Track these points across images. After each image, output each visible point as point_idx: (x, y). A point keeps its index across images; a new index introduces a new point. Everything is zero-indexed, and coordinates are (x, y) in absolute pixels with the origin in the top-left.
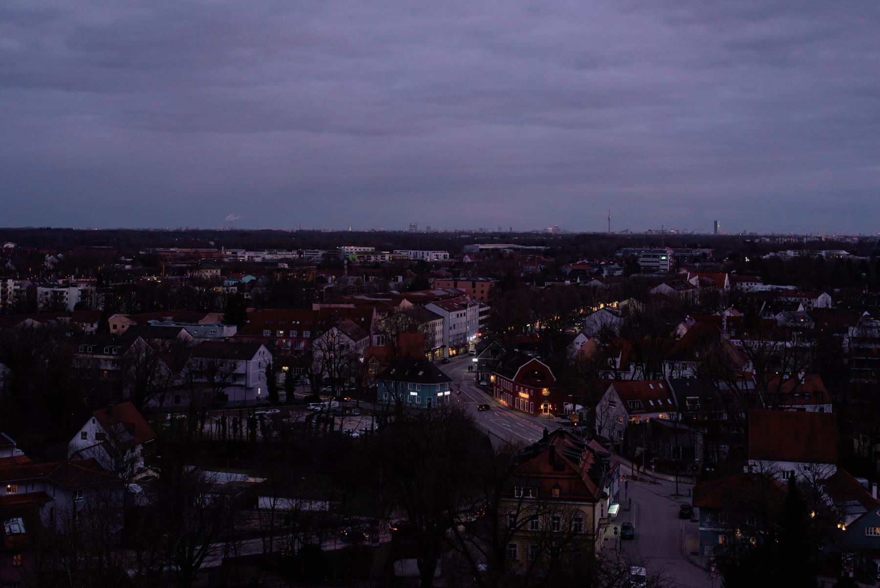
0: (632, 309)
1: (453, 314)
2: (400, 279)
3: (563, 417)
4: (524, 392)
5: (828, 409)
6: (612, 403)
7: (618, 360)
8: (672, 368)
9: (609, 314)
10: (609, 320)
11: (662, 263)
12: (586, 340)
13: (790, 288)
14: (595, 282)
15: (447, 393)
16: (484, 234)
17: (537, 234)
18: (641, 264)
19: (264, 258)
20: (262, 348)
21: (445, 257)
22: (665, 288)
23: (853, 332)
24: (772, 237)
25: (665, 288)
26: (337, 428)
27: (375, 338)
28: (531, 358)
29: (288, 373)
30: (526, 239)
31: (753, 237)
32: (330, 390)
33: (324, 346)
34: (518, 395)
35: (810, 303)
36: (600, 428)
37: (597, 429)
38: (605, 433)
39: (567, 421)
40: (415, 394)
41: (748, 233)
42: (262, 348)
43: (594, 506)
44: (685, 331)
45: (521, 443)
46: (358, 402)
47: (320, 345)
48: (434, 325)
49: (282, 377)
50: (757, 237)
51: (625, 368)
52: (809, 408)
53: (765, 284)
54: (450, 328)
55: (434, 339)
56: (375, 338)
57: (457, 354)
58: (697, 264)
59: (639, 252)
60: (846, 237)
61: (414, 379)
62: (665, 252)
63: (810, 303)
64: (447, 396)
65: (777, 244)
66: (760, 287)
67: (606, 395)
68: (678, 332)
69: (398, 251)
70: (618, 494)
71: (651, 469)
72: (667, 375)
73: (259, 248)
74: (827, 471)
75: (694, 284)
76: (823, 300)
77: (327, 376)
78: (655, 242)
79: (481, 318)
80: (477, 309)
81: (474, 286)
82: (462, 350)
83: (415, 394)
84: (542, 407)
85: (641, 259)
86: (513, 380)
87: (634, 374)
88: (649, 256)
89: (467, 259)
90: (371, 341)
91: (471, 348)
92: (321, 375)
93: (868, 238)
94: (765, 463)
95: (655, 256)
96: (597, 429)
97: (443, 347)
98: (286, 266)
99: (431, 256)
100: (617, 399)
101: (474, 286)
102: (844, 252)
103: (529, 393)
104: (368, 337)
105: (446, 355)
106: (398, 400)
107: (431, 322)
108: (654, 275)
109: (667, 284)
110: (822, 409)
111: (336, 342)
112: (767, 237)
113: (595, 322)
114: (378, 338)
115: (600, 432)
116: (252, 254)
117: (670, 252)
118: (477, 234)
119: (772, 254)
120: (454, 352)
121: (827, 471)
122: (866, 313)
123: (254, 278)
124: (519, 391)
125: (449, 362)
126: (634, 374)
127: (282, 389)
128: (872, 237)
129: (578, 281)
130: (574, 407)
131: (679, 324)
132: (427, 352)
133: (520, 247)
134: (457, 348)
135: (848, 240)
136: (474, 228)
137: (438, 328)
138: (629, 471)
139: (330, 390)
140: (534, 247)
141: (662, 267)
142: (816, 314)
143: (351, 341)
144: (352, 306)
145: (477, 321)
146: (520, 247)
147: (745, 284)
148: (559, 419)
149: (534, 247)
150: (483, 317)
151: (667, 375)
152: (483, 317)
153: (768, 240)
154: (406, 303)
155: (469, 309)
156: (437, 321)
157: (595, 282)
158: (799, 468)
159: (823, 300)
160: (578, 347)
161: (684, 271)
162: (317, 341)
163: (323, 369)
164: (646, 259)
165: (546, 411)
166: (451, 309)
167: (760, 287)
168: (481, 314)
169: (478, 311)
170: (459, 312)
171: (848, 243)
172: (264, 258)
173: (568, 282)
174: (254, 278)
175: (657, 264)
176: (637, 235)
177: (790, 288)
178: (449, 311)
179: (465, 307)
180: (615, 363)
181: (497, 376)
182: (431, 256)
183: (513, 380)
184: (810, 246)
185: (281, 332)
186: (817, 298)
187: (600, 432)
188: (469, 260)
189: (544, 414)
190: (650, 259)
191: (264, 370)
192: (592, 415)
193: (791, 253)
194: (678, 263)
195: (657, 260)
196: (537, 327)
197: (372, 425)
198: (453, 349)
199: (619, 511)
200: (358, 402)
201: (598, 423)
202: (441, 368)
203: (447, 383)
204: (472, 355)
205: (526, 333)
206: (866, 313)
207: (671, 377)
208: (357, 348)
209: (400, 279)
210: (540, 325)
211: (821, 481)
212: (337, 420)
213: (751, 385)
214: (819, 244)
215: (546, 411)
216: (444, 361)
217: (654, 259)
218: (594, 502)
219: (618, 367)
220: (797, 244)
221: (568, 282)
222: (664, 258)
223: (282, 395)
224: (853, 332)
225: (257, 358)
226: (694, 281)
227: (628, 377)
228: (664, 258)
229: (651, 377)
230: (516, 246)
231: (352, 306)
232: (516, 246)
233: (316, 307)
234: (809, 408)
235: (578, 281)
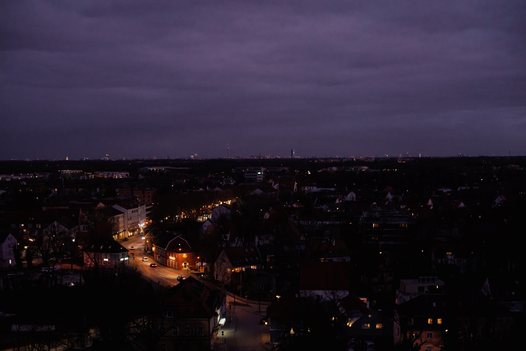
0: (238, 204)
1: (130, 211)
2: (98, 190)
3: (196, 270)
4: (172, 256)
5: (348, 259)
6: (223, 261)
7: (228, 235)
8: (260, 239)
9: (224, 208)
10: (225, 212)
11: (258, 176)
12: (210, 224)
13: (332, 189)
14: (217, 189)
15: (126, 259)
16: (151, 160)
17: (184, 160)
18: (246, 177)
19: (12, 179)
20: (10, 236)
21: (127, 175)
22: (258, 191)
23: (365, 214)
24: (325, 159)
25: (258, 191)
26: (58, 282)
27: (82, 227)
28: (176, 236)
29: (27, 250)
30: (179, 163)
31: (313, 159)
32: (55, 259)
33: (49, 233)
34: (168, 258)
35: (343, 198)
36: (217, 276)
37: (215, 276)
38: (220, 278)
39: (198, 272)
40: (107, 260)
41: (310, 157)
42: (10, 236)
43: (209, 321)
44: (268, 217)
45: (169, 286)
46: (72, 266)
47: (46, 232)
48: (119, 218)
49: (24, 253)
50: (317, 159)
51: (232, 240)
52: (335, 260)
53: (318, 188)
54: (128, 220)
55: (118, 226)
56: (82, 227)
57: (133, 235)
58: (279, 177)
59: (245, 170)
60: (368, 158)
61: (106, 252)
62: (260, 169)
63: (343, 198)
64: (126, 261)
65: (327, 163)
66: (315, 189)
67: (220, 256)
68: (265, 217)
69: (97, 172)
70: (225, 313)
71: (245, 297)
72: (256, 244)
73: (9, 173)
74: (342, 294)
75: (276, 188)
76: (351, 196)
77: (52, 251)
78: (256, 163)
79: (147, 213)
80: (145, 207)
81: (143, 193)
82: (136, 233)
83: (107, 260)
84: (183, 265)
85: (246, 174)
86: (166, 249)
87: (237, 243)
88: (250, 172)
89: (141, 177)
90: (79, 228)
91: (142, 231)
92: (48, 250)
93: (380, 158)
94: (308, 292)
95: (254, 172)
96: (215, 276)
97: (124, 231)
98: (25, 183)
99: (119, 176)
100: (227, 259)
101: (143, 193)
102: (366, 168)
103: (175, 257)
104: (77, 226)
105: (127, 236)
106: (96, 264)
107: (116, 216)
108: (253, 184)
109: (259, 189)
110: (344, 260)
111: (57, 230)
112: (321, 159)
113: (216, 213)
114: (84, 227)
115: (217, 278)
116: (4, 176)
117: (263, 169)
118: (147, 161)
119: (323, 169)
120: (131, 234)
121: (342, 294)
122: (375, 203)
123: (5, 192)
124: (169, 256)
125: (128, 240)
126: (237, 243)
127: (24, 260)
128: (382, 158)
129: (208, 188)
130: (202, 264)
131: (265, 213)
132: (115, 235)
133: (173, 168)
134: (133, 231)
135: (369, 160)
136: (146, 158)
137: (121, 220)
138: (232, 299)
139: (55, 259)
140: (182, 168)
141: (258, 179)
142: (346, 205)
143: (66, 229)
144: (67, 207)
145: (145, 214)
146: (173, 168)
147: (306, 188)
148: (193, 271)
149: (182, 168)
150: (149, 212)
151: (256, 244)
152: (149, 212)
153: (322, 161)
154: (101, 205)
155: (139, 207)
156: (120, 215)
157: (217, 189)
158: (326, 294)
159: (351, 196)
160: (206, 228)
161: (271, 181)
162: (44, 230)
163: (49, 247)
164: (249, 174)
165: (185, 267)
166: (128, 208)
167: (315, 189)
168: (147, 210)
169: (145, 208)
170: (134, 209)
171: (368, 162)
172: (12, 179)
173: (201, 189)
174: (5, 192)
175: (255, 177)
176: (245, 159)
177: (332, 189)
178: (128, 209)
179: (137, 206)
180: (226, 238)
181: (156, 248)
182: (119, 176)
183: (166, 249)
184: (344, 164)
185: (23, 225)
186: (347, 195)
187: (217, 278)
188: (142, 177)
189: (184, 268)
190: (251, 174)
191: (12, 249)
192: (212, 269)
193: (335, 169)
194: (267, 176)
195: (255, 174)
196: (182, 217)
197: (80, 279)
198: (130, 232)
199: (226, 323)
200: (72, 266)
201: (215, 273)
202: (122, 244)
203: (126, 253)
204: (142, 235)
205: (175, 221)
206: (375, 203)
207: (259, 244)
208: (70, 234)
209: (98, 190)
210: (184, 216)
211: (339, 300)
212: (59, 277)
213: (303, 247)
214: (351, 163)
215: (185, 267)
216: (126, 240)
217: (253, 174)
218: (209, 318)
219: (228, 239)
220: (341, 163)
221: (201, 189)
222: (259, 173)
223: (25, 263)
224: (365, 214)
225: (7, 242)
226: (275, 187)
227: (234, 245)
228: (259, 173)
229: (247, 245)
230: (170, 168)
231: (67, 207)
232: (170, 168)
233: (44, 209)
234: (335, 260)
235: (208, 188)
